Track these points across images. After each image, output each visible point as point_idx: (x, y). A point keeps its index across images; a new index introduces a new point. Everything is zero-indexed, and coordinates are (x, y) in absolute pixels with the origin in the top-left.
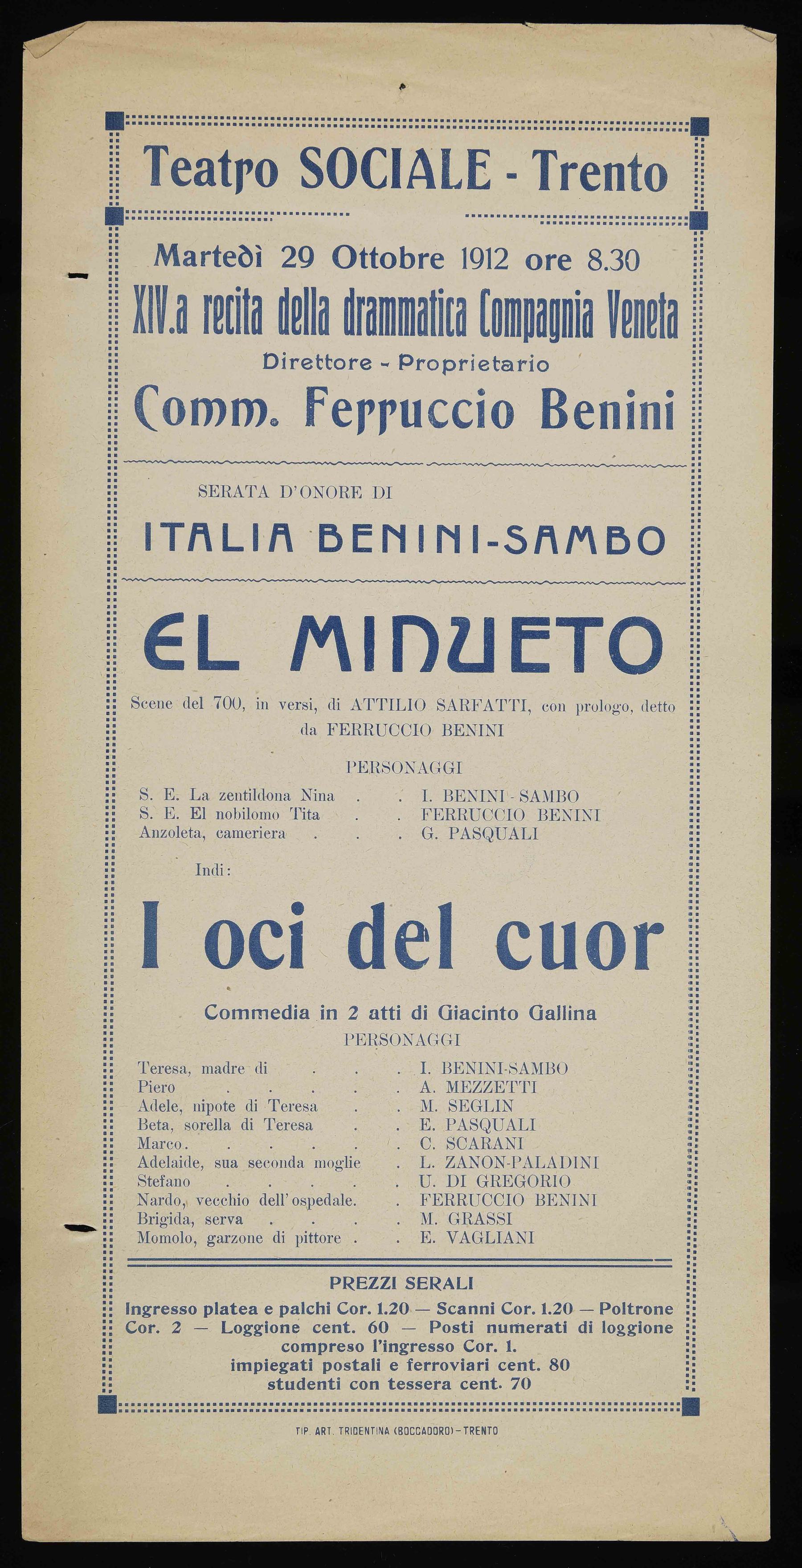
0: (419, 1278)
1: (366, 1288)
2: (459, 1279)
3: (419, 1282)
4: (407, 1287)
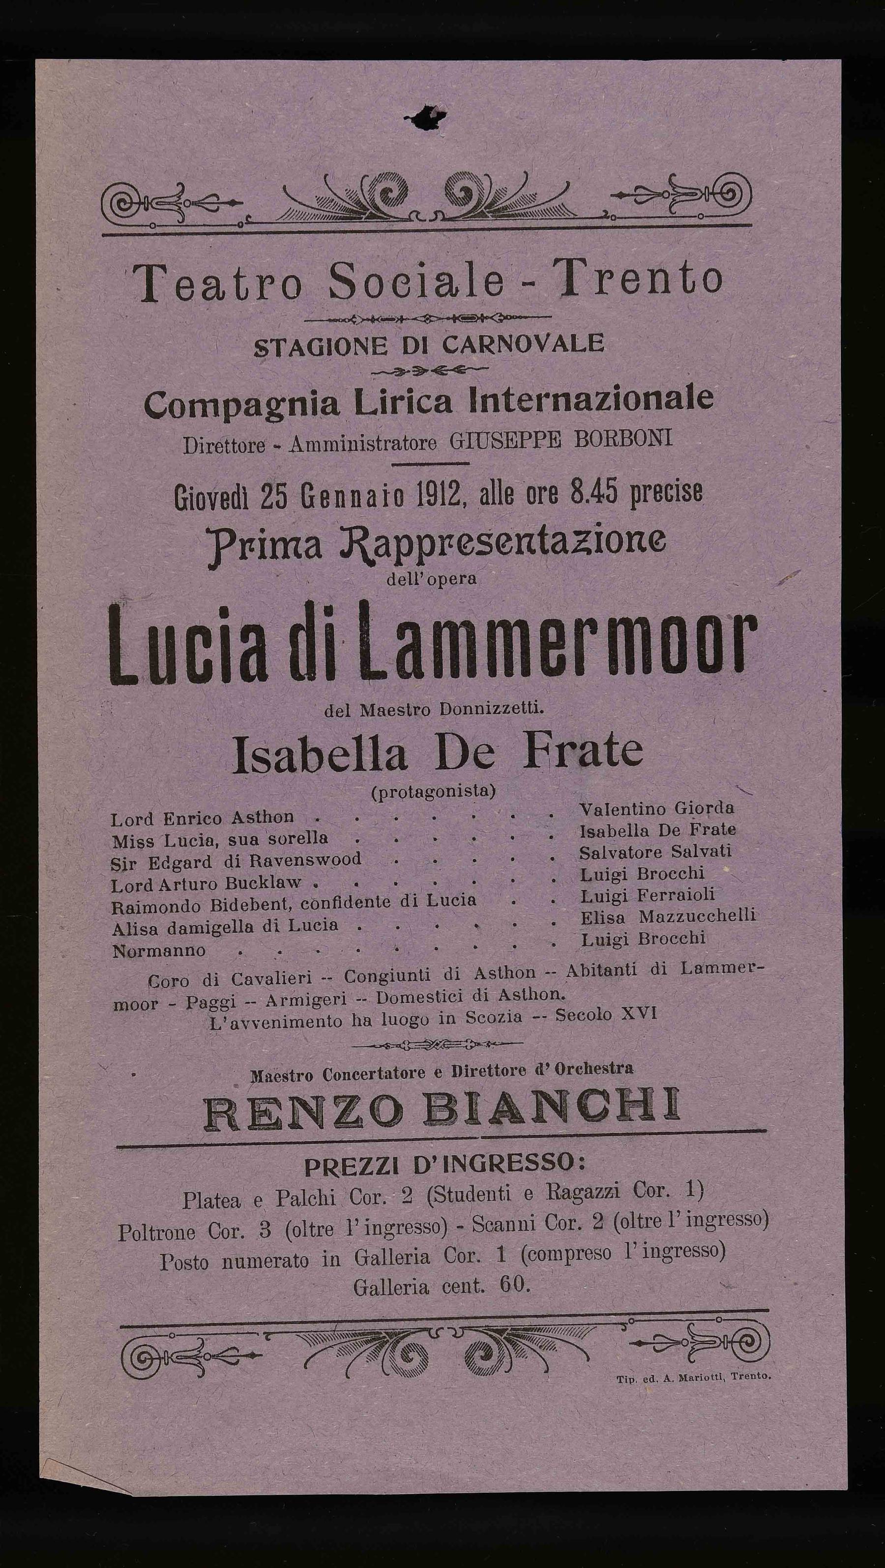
1: (355, 1174)
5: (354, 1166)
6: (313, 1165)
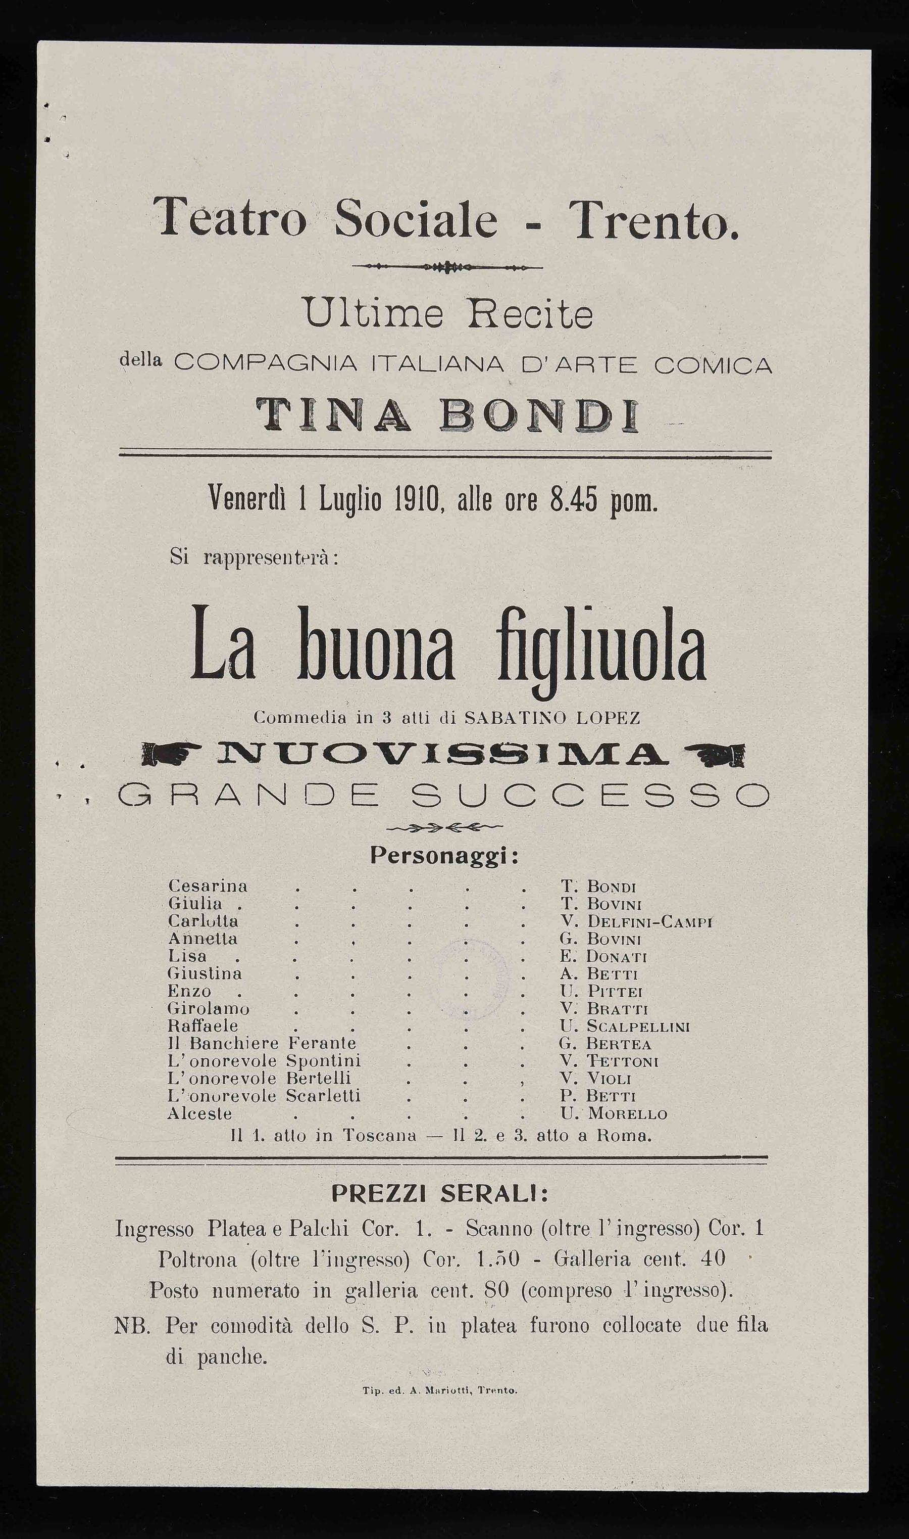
0: (460, 1186)
1: (381, 1201)
2: (516, 1187)
3: (461, 1192)
4: (443, 1199)
5: (381, 1193)
6: (340, 1190)
